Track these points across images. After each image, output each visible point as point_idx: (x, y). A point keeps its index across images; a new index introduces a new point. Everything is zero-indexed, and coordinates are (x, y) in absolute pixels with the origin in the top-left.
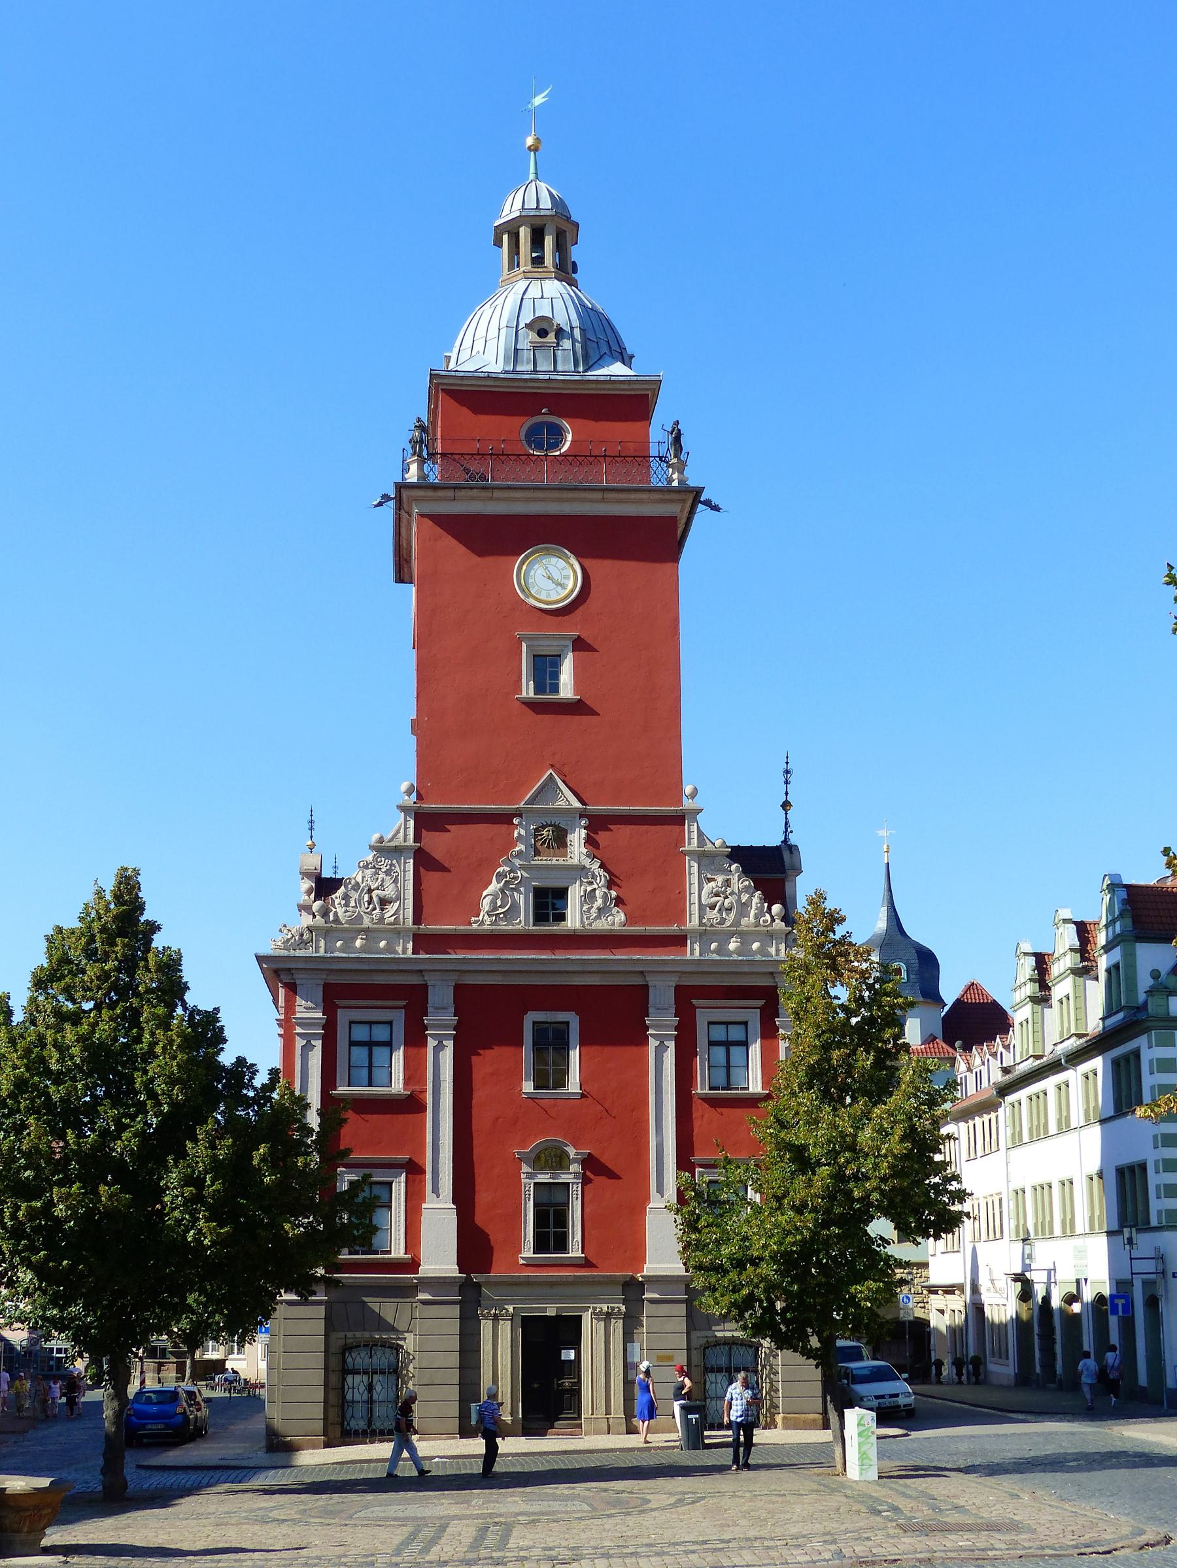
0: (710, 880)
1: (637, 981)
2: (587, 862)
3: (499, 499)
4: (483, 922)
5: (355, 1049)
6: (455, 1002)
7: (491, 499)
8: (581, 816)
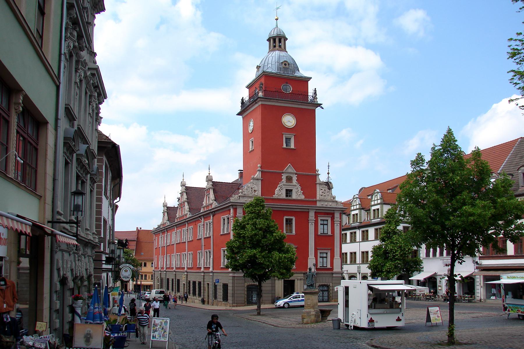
0: (321, 190)
1: (307, 211)
2: (297, 184)
3: (279, 102)
4: (275, 196)
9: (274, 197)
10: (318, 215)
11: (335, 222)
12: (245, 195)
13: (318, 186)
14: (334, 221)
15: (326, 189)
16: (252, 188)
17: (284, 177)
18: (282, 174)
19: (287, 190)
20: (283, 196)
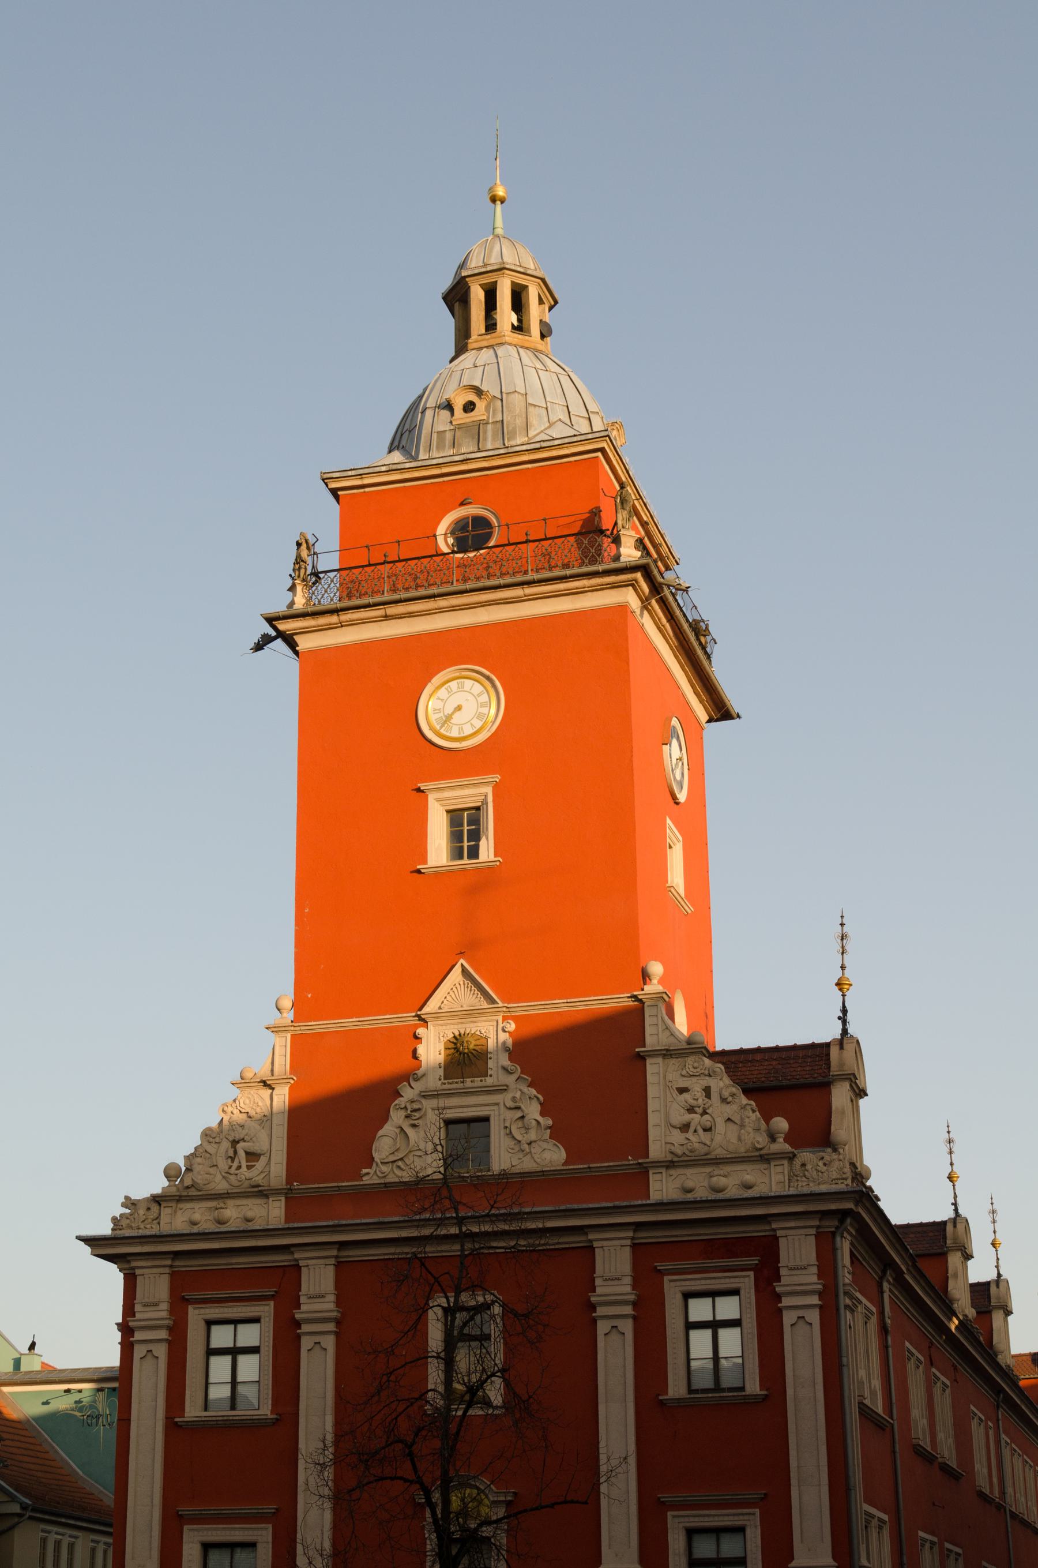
0: (682, 1090)
6: (337, 1288)
7: (387, 617)
9: (366, 1180)
10: (661, 1266)
12: (193, 1192)
13: (654, 1068)
14: (778, 1297)
15: (712, 1083)
16: (235, 1143)
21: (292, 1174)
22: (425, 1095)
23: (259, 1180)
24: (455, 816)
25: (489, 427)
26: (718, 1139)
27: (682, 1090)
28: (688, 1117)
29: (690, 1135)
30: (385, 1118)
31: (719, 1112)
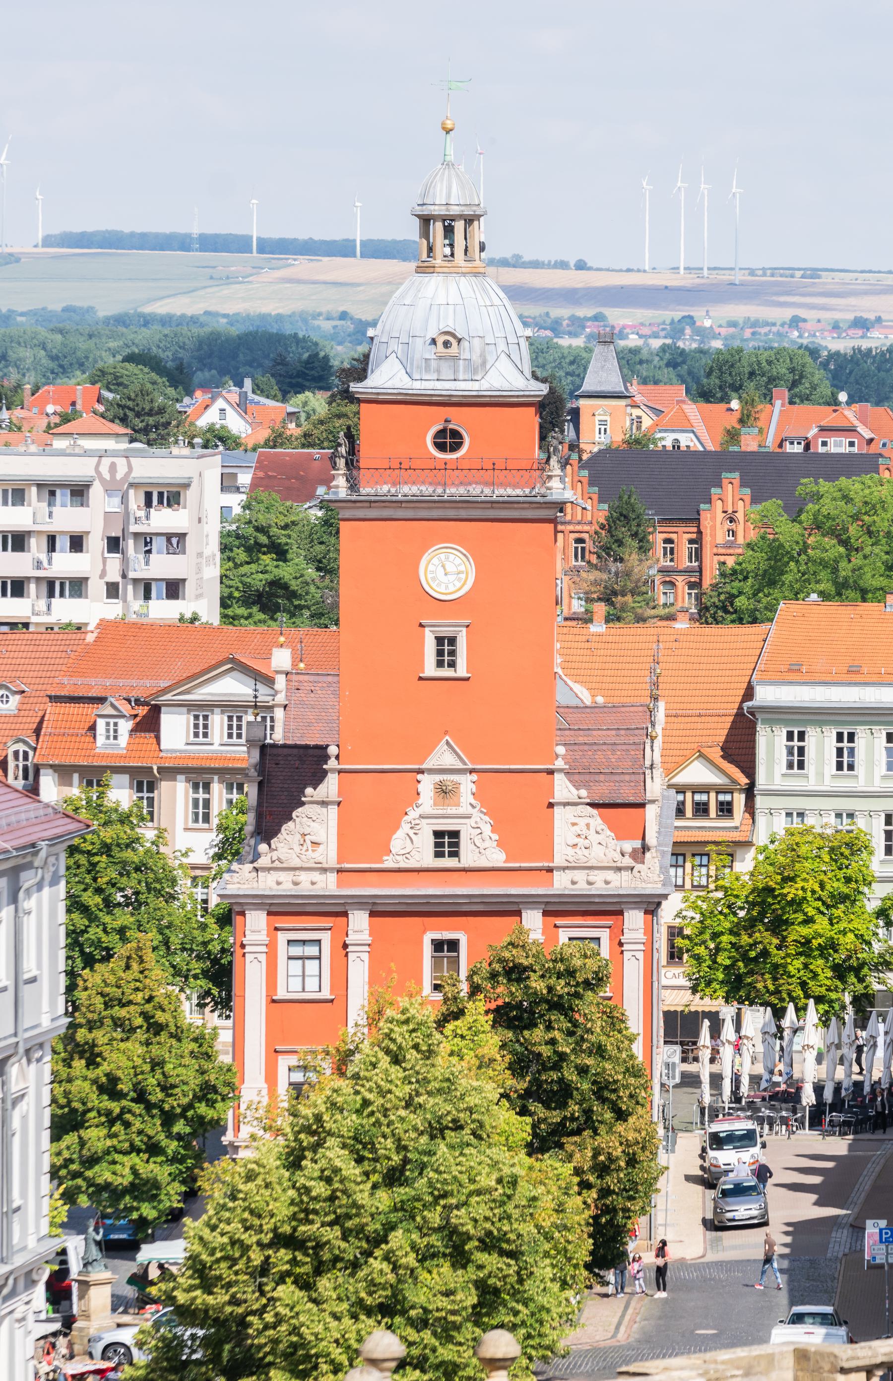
0: (574, 824)
2: (475, 812)
5: (291, 962)
8: (471, 772)
11: (626, 947)
17: (427, 783)
18: (420, 777)
19: (438, 834)
20: (424, 855)
21: (340, 859)
22: (422, 817)
23: (320, 859)
24: (440, 640)
25: (461, 362)
26: (593, 854)
27: (574, 824)
28: (577, 840)
29: (577, 850)
30: (397, 827)
31: (594, 838)
